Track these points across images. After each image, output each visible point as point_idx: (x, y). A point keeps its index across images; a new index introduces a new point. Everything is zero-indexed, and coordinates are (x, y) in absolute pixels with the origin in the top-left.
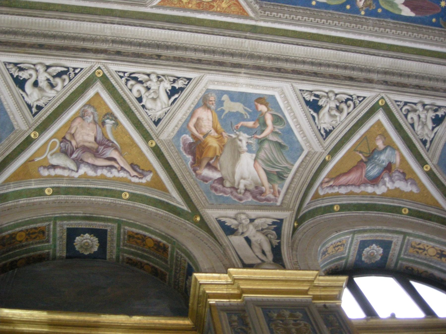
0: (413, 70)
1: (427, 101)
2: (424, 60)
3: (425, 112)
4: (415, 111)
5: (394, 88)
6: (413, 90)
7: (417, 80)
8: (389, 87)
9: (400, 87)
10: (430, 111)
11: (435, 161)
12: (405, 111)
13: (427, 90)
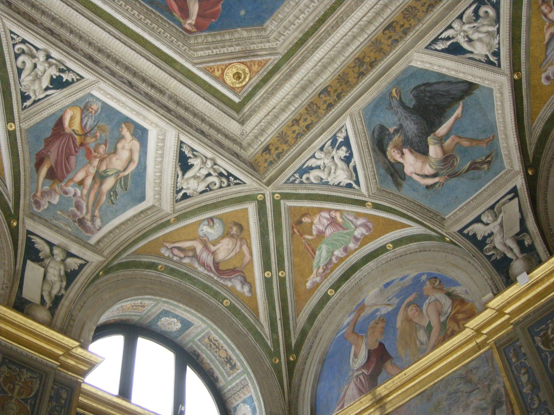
0: (52, 9)
1: (55, 54)
2: (73, 5)
3: (47, 65)
4: (33, 57)
5: (17, 16)
6: (42, 32)
7: (53, 24)
8: (10, 11)
9: (25, 18)
10: (53, 67)
11: (25, 126)
12: (18, 49)
13: (62, 42)
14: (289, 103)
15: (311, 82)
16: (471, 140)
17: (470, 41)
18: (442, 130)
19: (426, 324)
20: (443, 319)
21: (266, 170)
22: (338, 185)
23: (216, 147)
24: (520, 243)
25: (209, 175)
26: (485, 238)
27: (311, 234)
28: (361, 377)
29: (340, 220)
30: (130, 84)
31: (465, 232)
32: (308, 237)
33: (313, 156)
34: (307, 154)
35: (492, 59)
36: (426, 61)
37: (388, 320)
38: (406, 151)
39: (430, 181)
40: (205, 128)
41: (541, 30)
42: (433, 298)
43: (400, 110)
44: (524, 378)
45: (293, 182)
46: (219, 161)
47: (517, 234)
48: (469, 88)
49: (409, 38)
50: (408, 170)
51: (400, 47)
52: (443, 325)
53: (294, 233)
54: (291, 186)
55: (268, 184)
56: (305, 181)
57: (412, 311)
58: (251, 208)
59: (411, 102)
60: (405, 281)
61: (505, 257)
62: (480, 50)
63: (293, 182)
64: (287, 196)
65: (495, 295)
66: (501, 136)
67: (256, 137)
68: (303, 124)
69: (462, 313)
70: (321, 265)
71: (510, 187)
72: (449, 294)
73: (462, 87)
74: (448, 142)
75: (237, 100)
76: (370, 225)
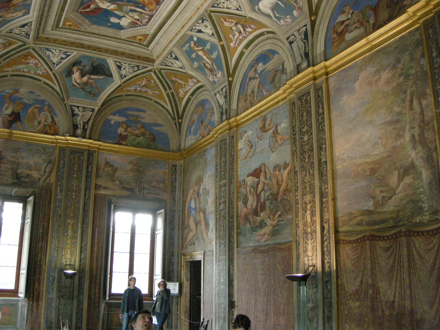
14: (70, 38)
15: (82, 40)
16: (97, 86)
17: (124, 69)
18: (93, 77)
19: (39, 120)
20: (46, 124)
21: (40, 41)
22: (51, 61)
23: (37, 29)
24: (84, 126)
25: (25, 32)
26: (76, 114)
27: (25, 60)
28: (6, 119)
29: (39, 66)
30: (45, 6)
31: (72, 107)
32: (24, 60)
33: (55, 50)
34: (55, 48)
35: (123, 76)
36: (111, 62)
37: (26, 106)
38: (79, 71)
39: (75, 84)
40: (43, 24)
41: (138, 81)
42: (46, 113)
43: (90, 63)
44: (62, 162)
45: (41, 49)
46: (32, 32)
47: (85, 122)
48: (111, 76)
49: (115, 56)
50: (74, 76)
51: (111, 55)
52: (45, 126)
53: (21, 56)
54: (40, 49)
55: (34, 44)
56: (45, 51)
57: (36, 111)
58: (20, 43)
59: (95, 64)
60: (39, 97)
61: (77, 125)
62: (123, 72)
63: (41, 49)
64: (34, 49)
65: (70, 136)
66: (103, 93)
67: (49, 34)
68: (65, 43)
69: (54, 128)
70: (16, 68)
71: (93, 107)
72: (52, 117)
73: (109, 74)
74: (91, 80)
75: (60, 26)
76: (45, 74)
